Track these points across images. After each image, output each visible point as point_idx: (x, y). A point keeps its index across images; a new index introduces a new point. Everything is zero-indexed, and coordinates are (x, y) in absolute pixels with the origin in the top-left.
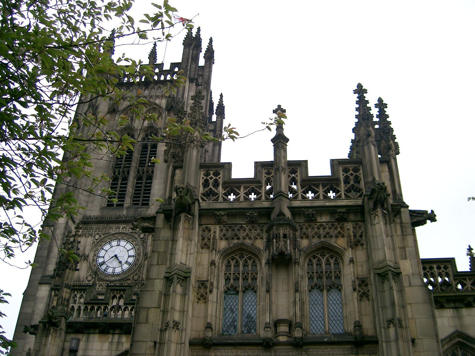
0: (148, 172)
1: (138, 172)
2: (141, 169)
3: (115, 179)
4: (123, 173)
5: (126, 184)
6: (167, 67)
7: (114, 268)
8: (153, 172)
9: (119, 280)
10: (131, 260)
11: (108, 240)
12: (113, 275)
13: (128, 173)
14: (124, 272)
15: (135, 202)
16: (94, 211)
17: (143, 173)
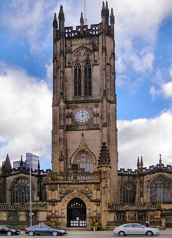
0: (89, 81)
1: (85, 81)
2: (86, 79)
4: (78, 82)
5: (81, 86)
6: (89, 28)
7: (82, 121)
8: (91, 81)
9: (85, 125)
10: (88, 117)
11: (78, 110)
12: (83, 123)
13: (81, 82)
15: (86, 94)
16: (70, 99)
17: (87, 81)
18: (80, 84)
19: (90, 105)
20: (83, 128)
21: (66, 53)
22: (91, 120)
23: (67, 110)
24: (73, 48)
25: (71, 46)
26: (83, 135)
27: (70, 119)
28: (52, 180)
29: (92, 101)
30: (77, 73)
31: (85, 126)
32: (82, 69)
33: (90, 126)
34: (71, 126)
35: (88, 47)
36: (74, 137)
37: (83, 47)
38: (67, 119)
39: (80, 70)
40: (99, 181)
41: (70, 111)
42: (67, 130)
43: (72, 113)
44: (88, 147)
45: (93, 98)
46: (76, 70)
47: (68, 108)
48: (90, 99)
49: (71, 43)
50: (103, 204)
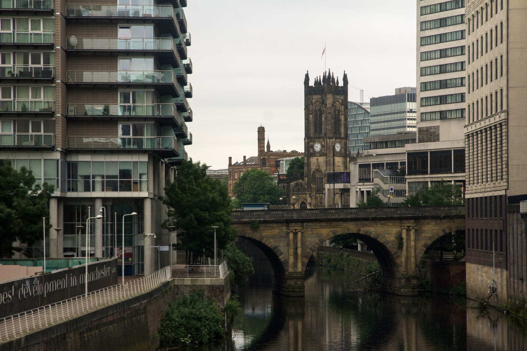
3: (315, 125)
12: (317, 152)
14: (319, 151)
16: (312, 136)
18: (317, 125)
19: (321, 140)
20: (318, 155)
21: (310, 105)
22: (321, 150)
23: (310, 143)
24: (314, 101)
25: (312, 100)
26: (317, 159)
27: (312, 149)
28: (293, 191)
29: (321, 138)
30: (315, 117)
31: (319, 154)
32: (318, 115)
33: (321, 154)
34: (312, 153)
35: (320, 100)
36: (313, 160)
37: (317, 101)
38: (311, 149)
39: (317, 115)
40: (310, 193)
41: (312, 143)
42: (311, 156)
43: (313, 145)
44: (320, 167)
45: (322, 136)
46: (315, 115)
47: (311, 142)
48: (321, 136)
49: (312, 98)
50: (312, 205)
